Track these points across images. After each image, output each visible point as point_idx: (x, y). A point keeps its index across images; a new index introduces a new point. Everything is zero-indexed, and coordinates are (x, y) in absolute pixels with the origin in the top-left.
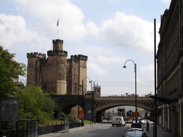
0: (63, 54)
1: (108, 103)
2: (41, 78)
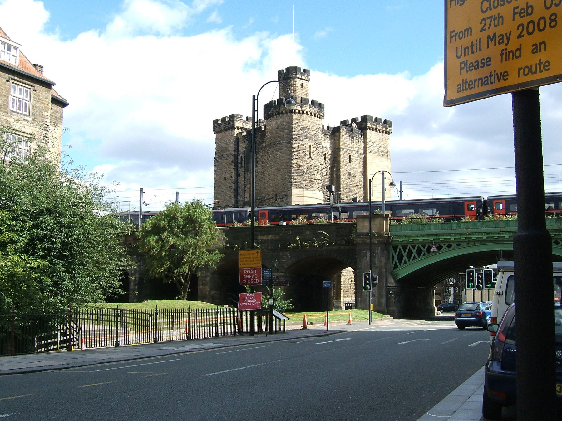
0: (307, 109)
1: (439, 248)
2: (248, 186)
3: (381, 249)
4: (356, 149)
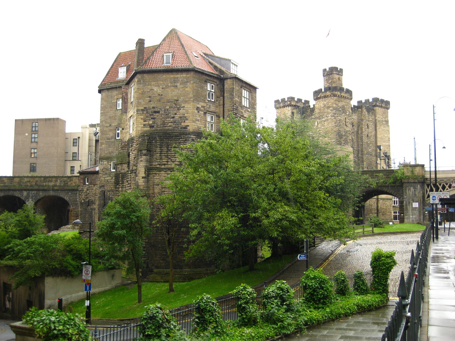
3: (420, 186)
4: (371, 119)
